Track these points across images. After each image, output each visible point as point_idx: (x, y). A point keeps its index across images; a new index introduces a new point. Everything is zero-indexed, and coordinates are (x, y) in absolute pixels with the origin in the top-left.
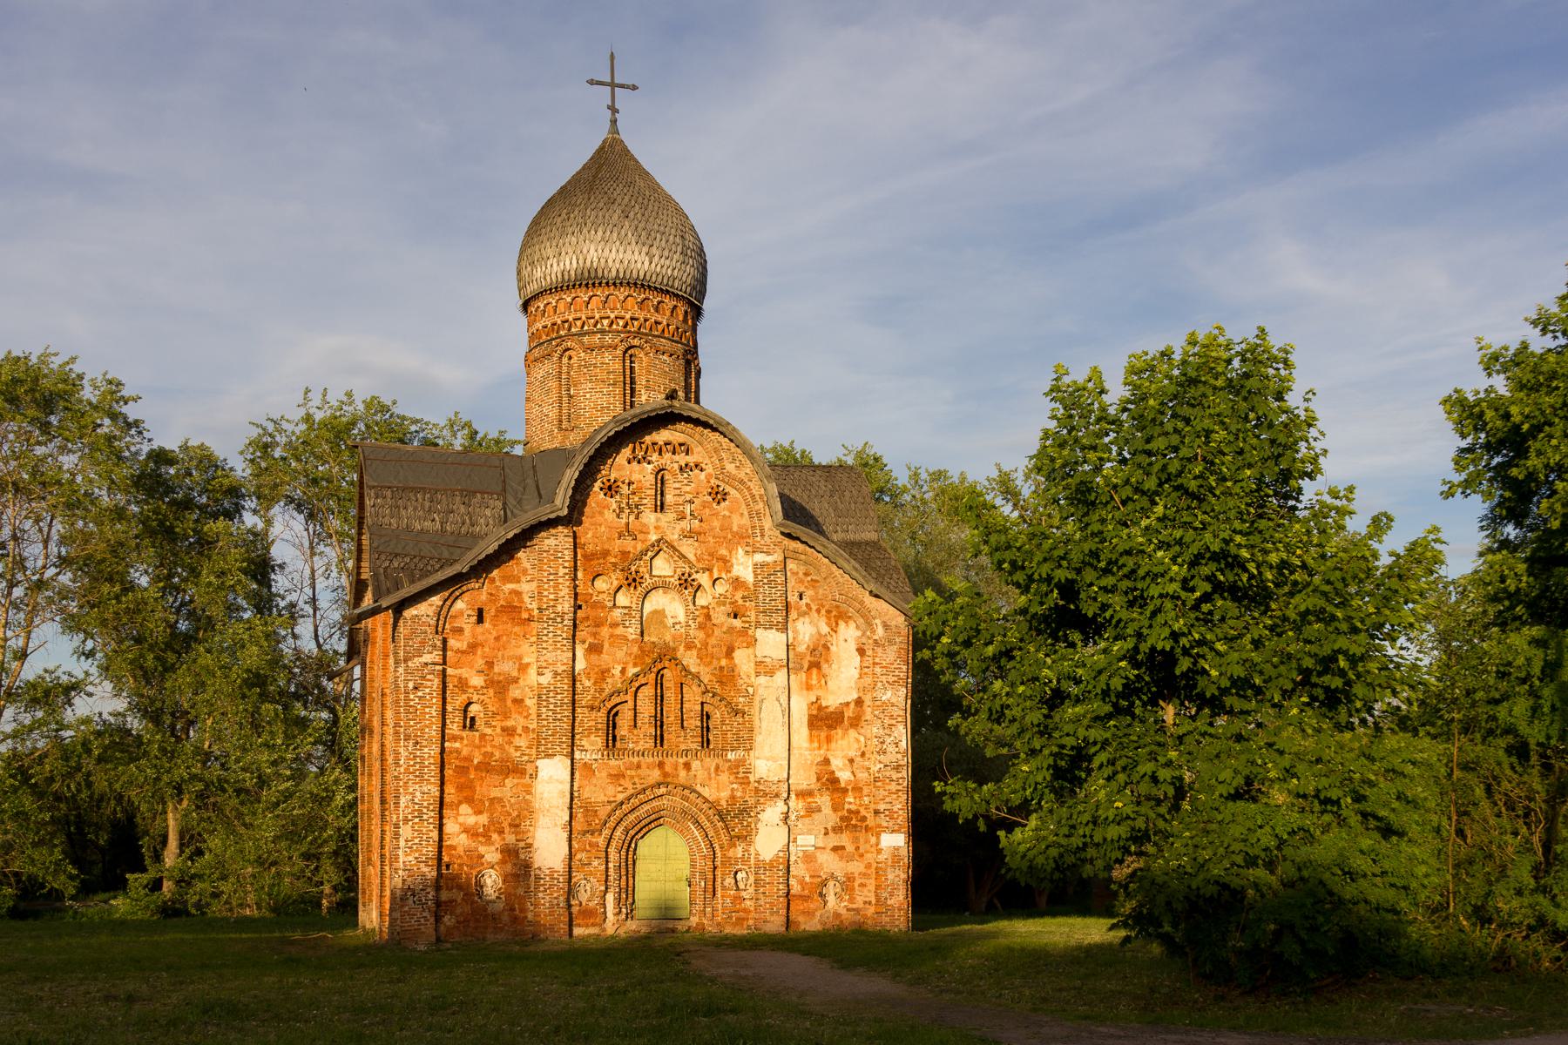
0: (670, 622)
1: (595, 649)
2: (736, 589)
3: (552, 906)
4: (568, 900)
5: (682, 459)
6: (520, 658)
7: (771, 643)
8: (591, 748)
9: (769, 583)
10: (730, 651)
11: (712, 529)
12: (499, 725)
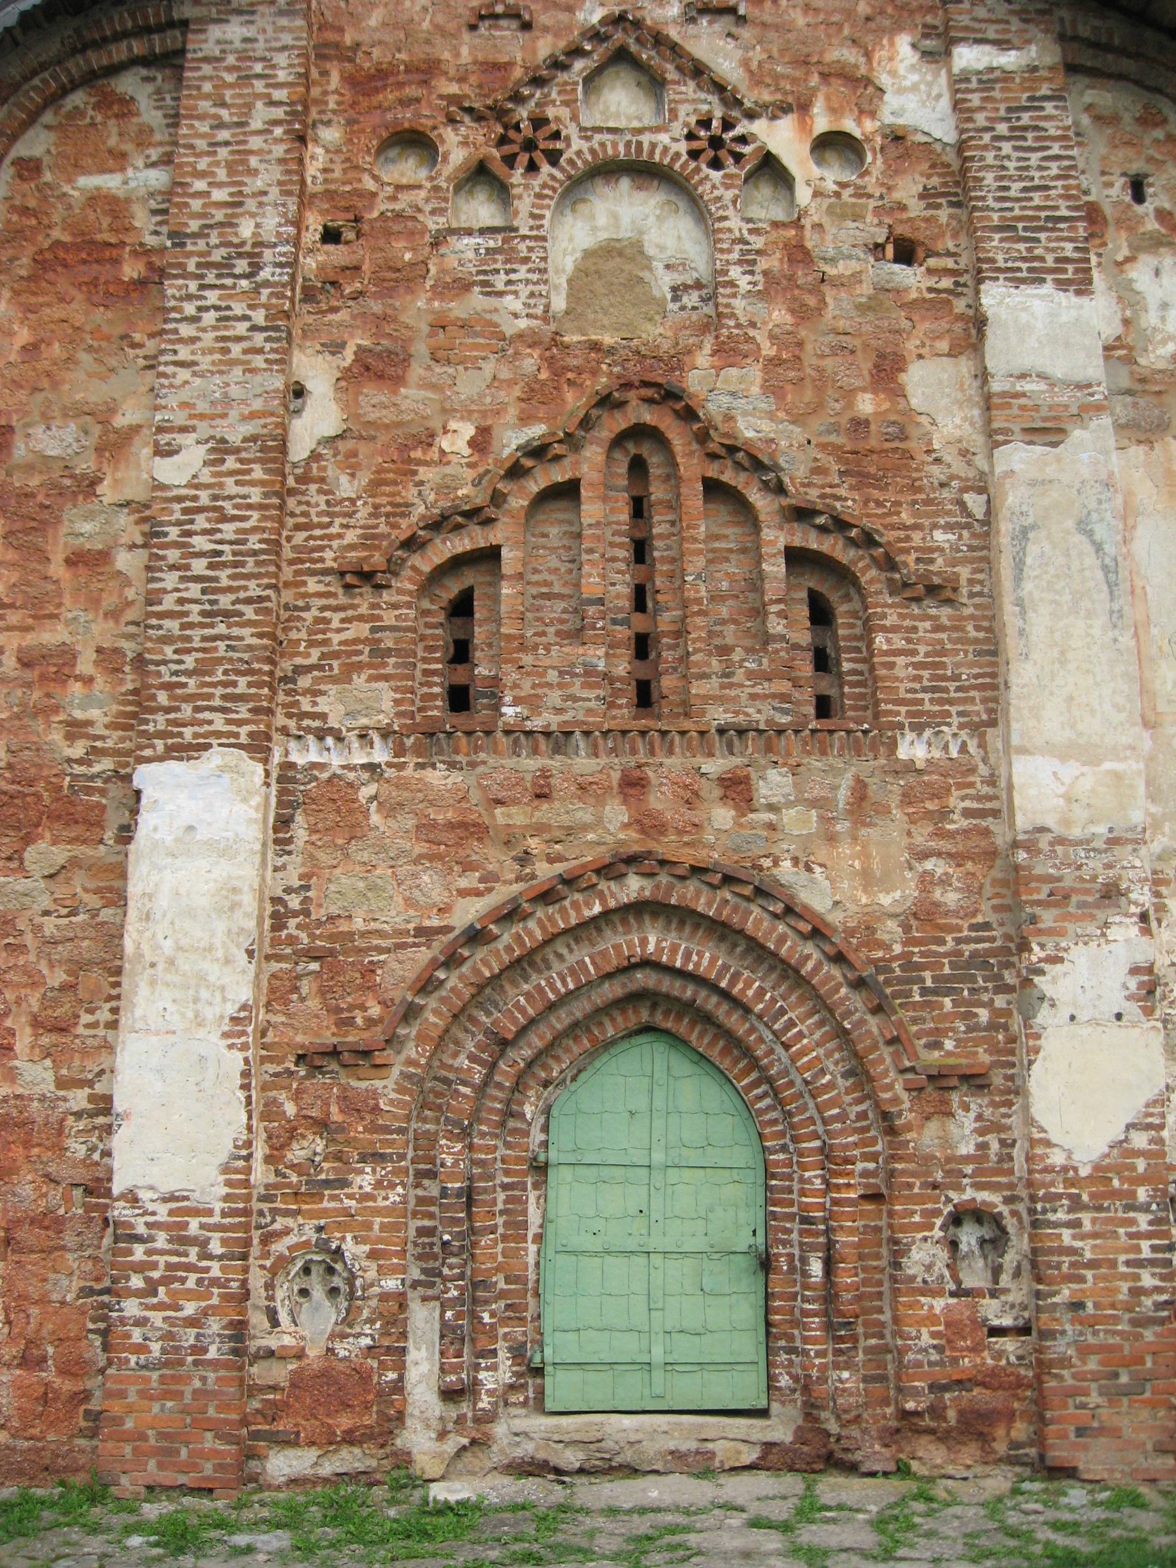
0: (663, 282)
1: (377, 368)
2: (894, 170)
4: (239, 1331)
6: (103, 415)
7: (1040, 328)
8: (357, 719)
10: (887, 371)
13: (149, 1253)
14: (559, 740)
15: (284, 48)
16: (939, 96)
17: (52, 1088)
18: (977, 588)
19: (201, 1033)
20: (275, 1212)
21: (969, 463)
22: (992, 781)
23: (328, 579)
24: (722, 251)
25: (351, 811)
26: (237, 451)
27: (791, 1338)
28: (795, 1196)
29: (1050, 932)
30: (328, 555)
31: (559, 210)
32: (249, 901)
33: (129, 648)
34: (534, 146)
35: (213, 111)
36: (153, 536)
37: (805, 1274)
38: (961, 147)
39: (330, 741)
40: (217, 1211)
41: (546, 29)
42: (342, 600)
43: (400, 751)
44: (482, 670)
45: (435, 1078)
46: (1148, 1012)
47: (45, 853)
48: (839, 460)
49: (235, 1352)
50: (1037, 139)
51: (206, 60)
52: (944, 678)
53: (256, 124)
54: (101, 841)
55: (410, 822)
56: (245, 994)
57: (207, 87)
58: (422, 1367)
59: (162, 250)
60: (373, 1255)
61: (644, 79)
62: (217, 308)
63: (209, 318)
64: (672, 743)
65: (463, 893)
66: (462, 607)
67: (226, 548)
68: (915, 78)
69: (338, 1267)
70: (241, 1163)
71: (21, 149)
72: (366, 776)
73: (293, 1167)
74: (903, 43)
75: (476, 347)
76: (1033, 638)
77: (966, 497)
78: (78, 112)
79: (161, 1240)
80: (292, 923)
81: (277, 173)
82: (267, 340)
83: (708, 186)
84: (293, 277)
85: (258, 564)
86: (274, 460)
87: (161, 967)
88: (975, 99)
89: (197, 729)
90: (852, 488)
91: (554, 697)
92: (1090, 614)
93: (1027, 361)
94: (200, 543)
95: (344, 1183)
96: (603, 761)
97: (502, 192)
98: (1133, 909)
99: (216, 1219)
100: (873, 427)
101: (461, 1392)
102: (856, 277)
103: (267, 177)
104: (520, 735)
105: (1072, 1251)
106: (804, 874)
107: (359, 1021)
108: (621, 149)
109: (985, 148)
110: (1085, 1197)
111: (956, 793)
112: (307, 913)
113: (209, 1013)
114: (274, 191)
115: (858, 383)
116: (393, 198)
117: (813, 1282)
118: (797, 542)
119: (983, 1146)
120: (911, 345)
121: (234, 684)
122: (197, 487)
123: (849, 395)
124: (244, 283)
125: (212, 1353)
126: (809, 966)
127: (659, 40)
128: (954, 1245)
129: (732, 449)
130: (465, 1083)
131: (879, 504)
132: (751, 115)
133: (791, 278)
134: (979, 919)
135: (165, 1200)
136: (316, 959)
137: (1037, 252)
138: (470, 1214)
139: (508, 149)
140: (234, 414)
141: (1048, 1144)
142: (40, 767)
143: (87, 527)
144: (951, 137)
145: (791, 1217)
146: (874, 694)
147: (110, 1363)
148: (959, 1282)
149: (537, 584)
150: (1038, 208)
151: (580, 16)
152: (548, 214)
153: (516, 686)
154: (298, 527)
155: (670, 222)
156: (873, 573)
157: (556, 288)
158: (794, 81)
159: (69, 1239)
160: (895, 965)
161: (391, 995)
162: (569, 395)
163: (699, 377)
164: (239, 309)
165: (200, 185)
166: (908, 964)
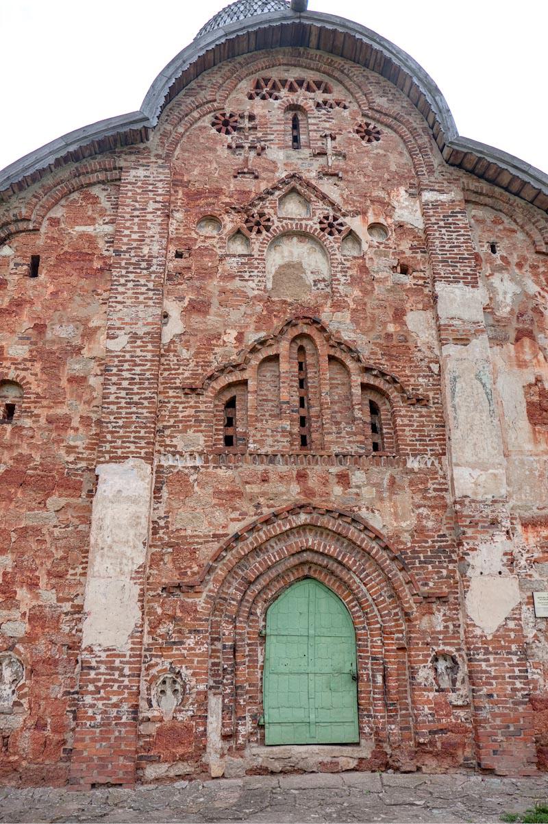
0: (310, 279)
1: (198, 308)
3: (105, 724)
4: (135, 709)
5: (320, 96)
7: (460, 301)
9: (447, 225)
10: (399, 315)
11: (362, 169)
12: (44, 413)
13: (97, 674)
14: (272, 458)
15: (161, 181)
16: (417, 210)
17: (55, 602)
18: (436, 401)
19: (123, 578)
20: (152, 656)
21: (432, 352)
22: (444, 477)
23: (178, 391)
24: (334, 267)
25: (186, 485)
26: (142, 338)
27: (369, 711)
28: (369, 649)
29: (471, 538)
30: (178, 381)
31: (269, 249)
32: (144, 522)
33: (94, 417)
34: (259, 224)
35: (132, 203)
36: (106, 370)
37: (374, 682)
38: (425, 231)
39: (178, 456)
40: (128, 655)
41: (264, 179)
42: (183, 399)
43: (207, 461)
44: (240, 429)
45: (220, 598)
46: (512, 571)
47: (55, 501)
48: (381, 349)
49: (134, 719)
50: (455, 228)
51: (129, 183)
52: (424, 436)
53: (150, 210)
54: (80, 496)
55: (211, 491)
56: (141, 560)
57: (130, 194)
58: (214, 725)
59: (110, 257)
60: (194, 674)
61: (302, 200)
62: (134, 281)
63: (130, 285)
64: (317, 460)
65: (232, 520)
66: (231, 404)
67: (137, 377)
68: (407, 203)
69: (179, 680)
70: (139, 634)
71: (51, 214)
72: (193, 471)
73: (160, 636)
74: (402, 190)
75: (237, 301)
76: (460, 420)
77: (431, 365)
78: (75, 201)
79: (103, 669)
80: (161, 532)
81: (158, 229)
82: (154, 294)
83: (328, 242)
84: (164, 270)
85: (149, 383)
86: (156, 342)
87: (106, 549)
88: (431, 212)
89: (123, 450)
90: (386, 361)
91: (270, 441)
92: (481, 411)
93: (453, 313)
94: (126, 374)
95: (182, 643)
96: (289, 467)
97: (247, 240)
98: (503, 529)
99: (127, 659)
100: (394, 337)
101: (230, 736)
102: (386, 279)
103: (154, 230)
104: (256, 456)
105: (486, 672)
106: (372, 514)
107: (189, 573)
108: (294, 226)
109: (435, 231)
110: (490, 649)
111: (430, 482)
112: (168, 528)
113: (126, 569)
114: (157, 236)
115: (388, 320)
116: (204, 241)
117: (377, 684)
118: (365, 381)
119: (447, 627)
120: (408, 306)
121: (139, 432)
122: (124, 352)
123: (384, 324)
124: (145, 271)
125: (124, 720)
126: (374, 551)
127: (308, 185)
128: (436, 669)
129: (340, 344)
130: (233, 599)
131: (397, 367)
132: (344, 215)
133: (361, 278)
134: (441, 533)
135: (105, 651)
136: (171, 547)
137: (457, 271)
138: (235, 656)
139: (250, 225)
140: (140, 323)
141: (474, 626)
142: (55, 465)
143: (77, 367)
144: (422, 226)
145: (367, 658)
146: (397, 442)
147: (77, 725)
148: (439, 686)
149: (262, 395)
150: (456, 254)
151: (277, 174)
152: (265, 250)
153: (254, 436)
154: (165, 370)
155: (313, 255)
156: (396, 394)
157: (268, 279)
158: (360, 203)
159: (60, 669)
160: (408, 551)
161: (202, 562)
162: (275, 321)
163: (325, 316)
164: (143, 281)
165: (127, 232)
166: (414, 551)
